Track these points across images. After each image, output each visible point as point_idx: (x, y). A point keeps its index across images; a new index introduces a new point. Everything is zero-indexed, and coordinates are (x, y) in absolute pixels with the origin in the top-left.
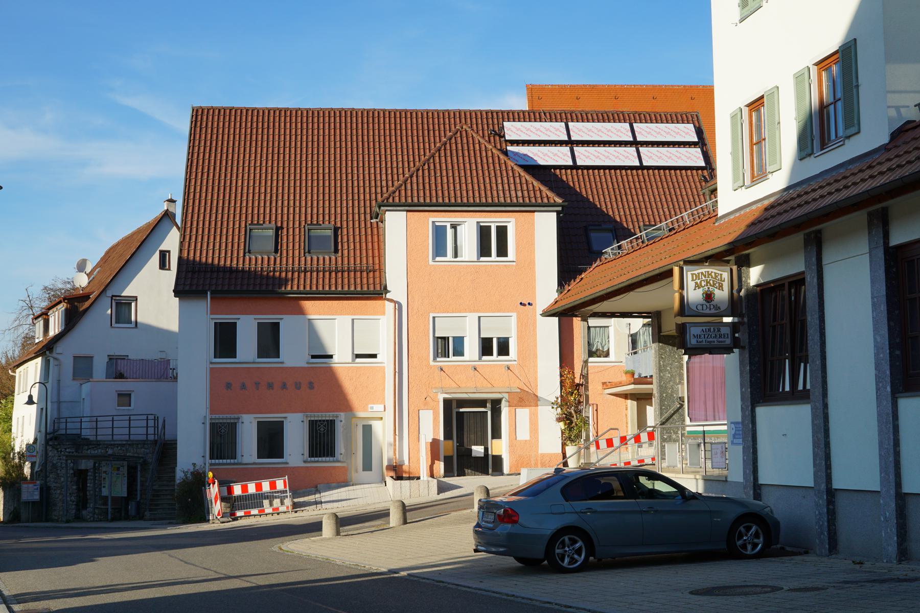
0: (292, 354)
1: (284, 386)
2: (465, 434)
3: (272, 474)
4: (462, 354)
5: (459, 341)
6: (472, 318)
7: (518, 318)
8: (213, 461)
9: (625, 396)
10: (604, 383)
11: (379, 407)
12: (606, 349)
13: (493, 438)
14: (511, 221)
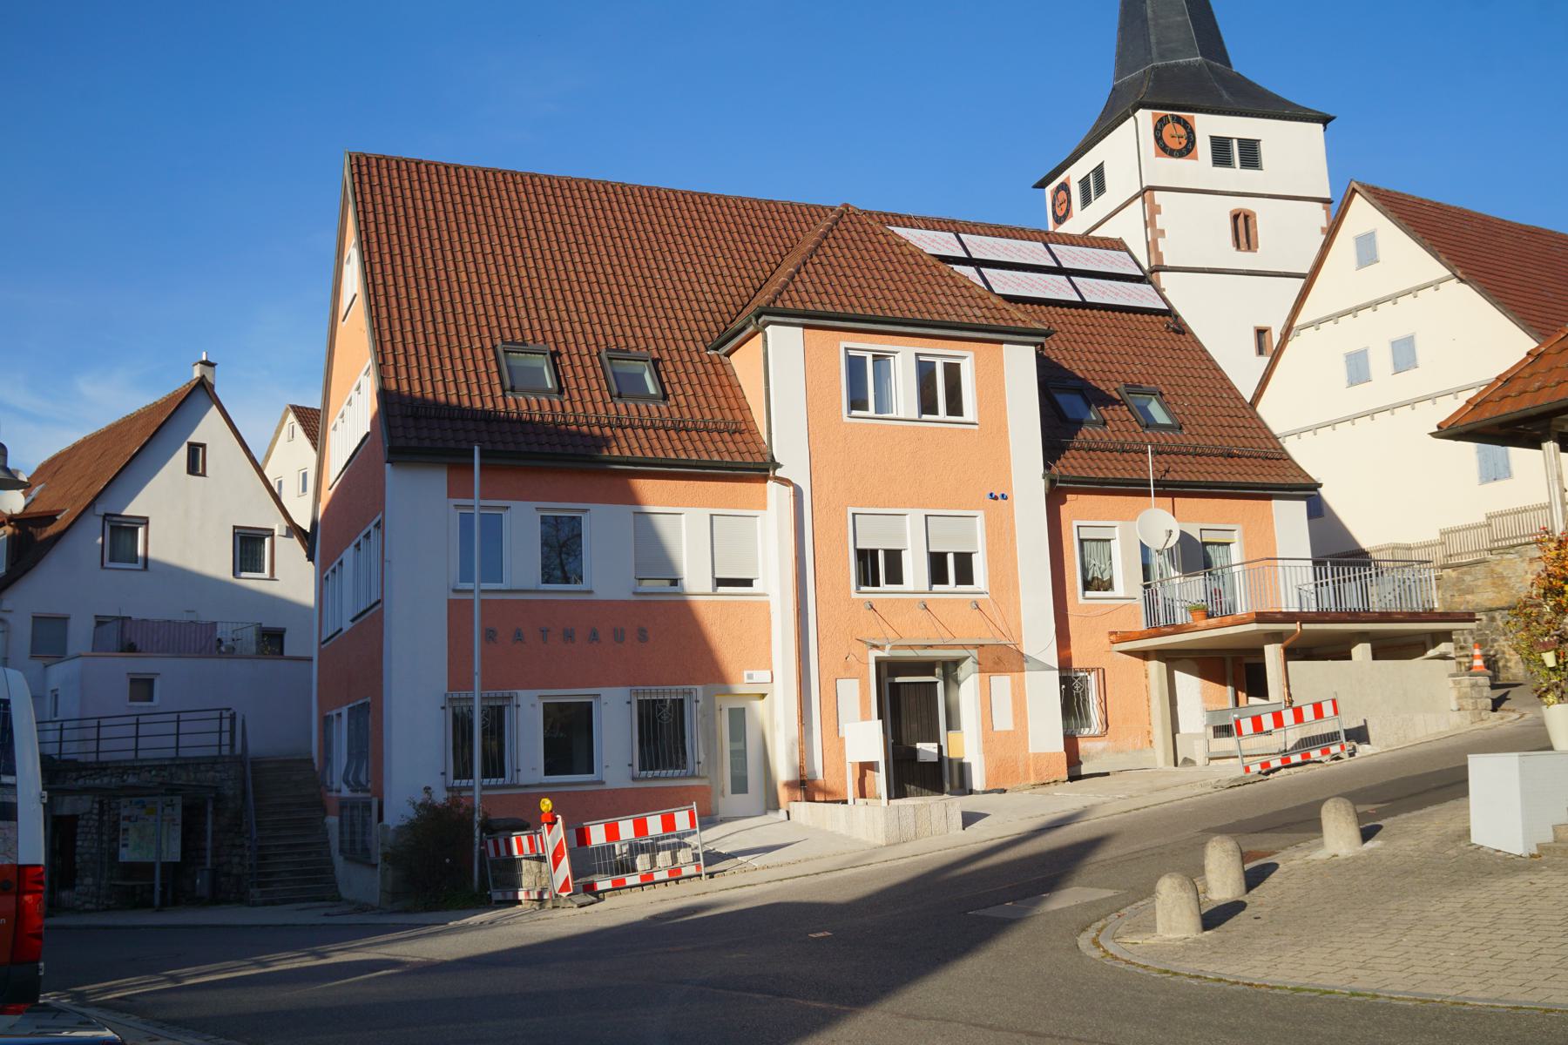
0: (606, 575)
1: (594, 636)
2: (904, 721)
3: (665, 802)
4: (899, 581)
5: (894, 557)
6: (912, 522)
7: (987, 519)
8: (486, 781)
9: (1145, 655)
10: (1111, 633)
11: (761, 676)
13: (949, 728)
14: (969, 359)
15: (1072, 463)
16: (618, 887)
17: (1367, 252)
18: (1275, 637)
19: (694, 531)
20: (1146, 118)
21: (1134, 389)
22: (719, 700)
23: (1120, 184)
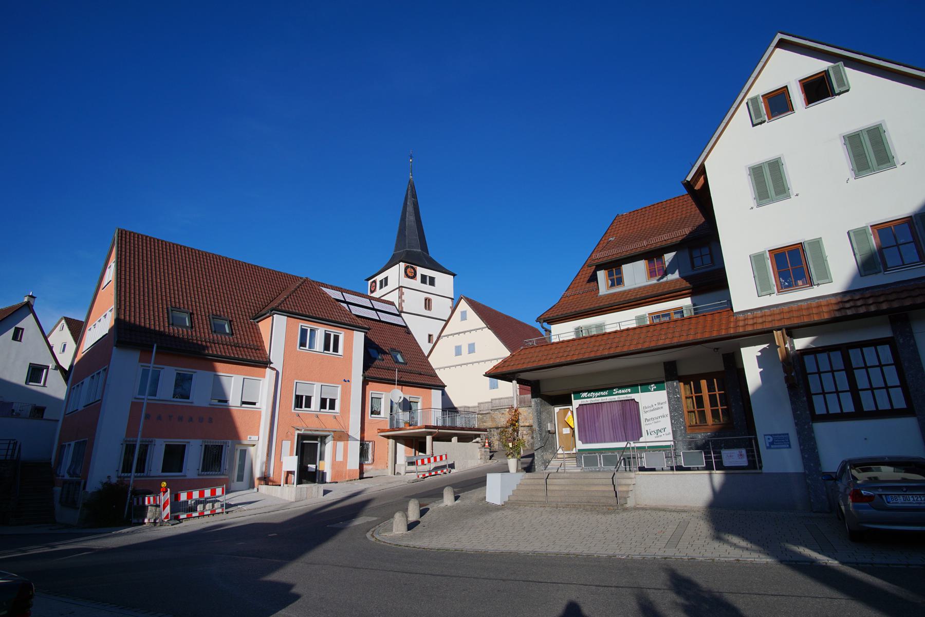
0: (199, 397)
1: (191, 419)
3: (213, 484)
5: (309, 399)
9: (388, 437)
11: (255, 438)
14: (342, 335)
15: (372, 372)
16: (189, 517)
17: (464, 316)
18: (430, 433)
19: (235, 383)
20: (402, 265)
21: (393, 350)
22: (237, 446)
23: (392, 284)
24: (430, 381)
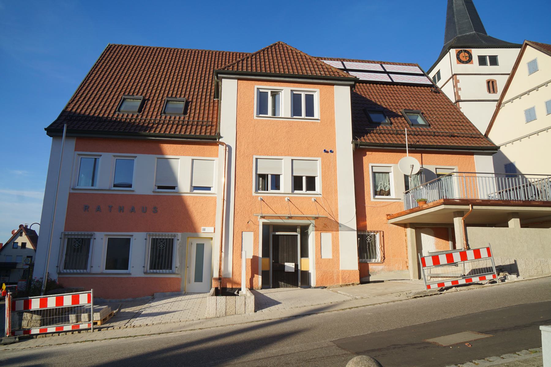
1: (133, 210)
5: (276, 179)
6: (286, 161)
9: (405, 225)
10: (388, 215)
11: (210, 229)
12: (387, 190)
13: (302, 256)
14: (317, 92)
15: (369, 138)
16: (59, 332)
17: (533, 67)
18: (459, 213)
19: (187, 167)
20: (453, 52)
21: (408, 111)
22: (190, 240)
23: (445, 75)
24: (474, 144)
